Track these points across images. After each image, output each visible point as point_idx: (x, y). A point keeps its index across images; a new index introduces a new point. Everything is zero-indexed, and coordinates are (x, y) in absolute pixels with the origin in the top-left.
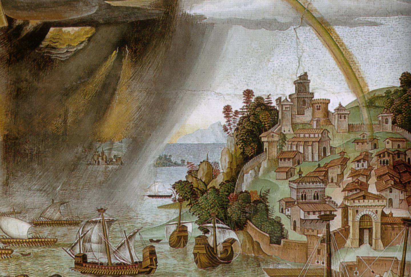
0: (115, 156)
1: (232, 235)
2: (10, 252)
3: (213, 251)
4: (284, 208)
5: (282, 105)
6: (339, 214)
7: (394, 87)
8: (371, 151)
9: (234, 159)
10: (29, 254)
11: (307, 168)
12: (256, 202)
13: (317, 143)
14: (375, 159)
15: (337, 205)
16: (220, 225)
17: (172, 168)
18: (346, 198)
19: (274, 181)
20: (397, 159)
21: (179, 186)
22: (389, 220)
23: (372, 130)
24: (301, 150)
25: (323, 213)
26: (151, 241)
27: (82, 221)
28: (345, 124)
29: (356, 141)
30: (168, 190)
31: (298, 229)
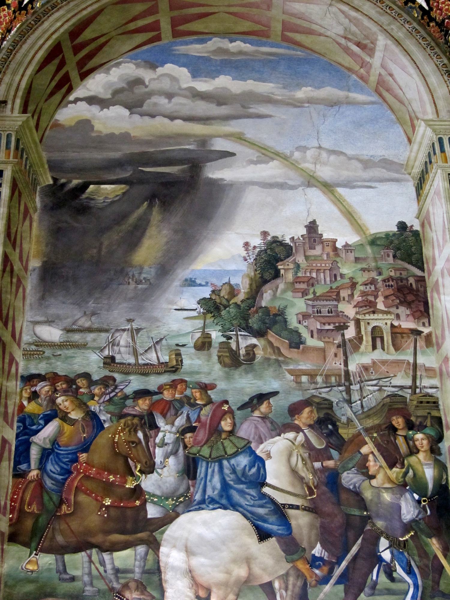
0: (144, 278)
1: (254, 341)
2: (41, 353)
4: (301, 319)
5: (295, 243)
6: (352, 326)
7: (391, 231)
8: (377, 278)
9: (254, 282)
10: (60, 355)
11: (320, 290)
12: (275, 315)
13: (328, 271)
14: (380, 284)
15: (350, 318)
16: (243, 333)
19: (291, 299)
20: (400, 284)
21: (203, 302)
24: (314, 275)
25: (337, 325)
26: (177, 345)
27: (111, 329)
28: (352, 256)
29: (363, 270)
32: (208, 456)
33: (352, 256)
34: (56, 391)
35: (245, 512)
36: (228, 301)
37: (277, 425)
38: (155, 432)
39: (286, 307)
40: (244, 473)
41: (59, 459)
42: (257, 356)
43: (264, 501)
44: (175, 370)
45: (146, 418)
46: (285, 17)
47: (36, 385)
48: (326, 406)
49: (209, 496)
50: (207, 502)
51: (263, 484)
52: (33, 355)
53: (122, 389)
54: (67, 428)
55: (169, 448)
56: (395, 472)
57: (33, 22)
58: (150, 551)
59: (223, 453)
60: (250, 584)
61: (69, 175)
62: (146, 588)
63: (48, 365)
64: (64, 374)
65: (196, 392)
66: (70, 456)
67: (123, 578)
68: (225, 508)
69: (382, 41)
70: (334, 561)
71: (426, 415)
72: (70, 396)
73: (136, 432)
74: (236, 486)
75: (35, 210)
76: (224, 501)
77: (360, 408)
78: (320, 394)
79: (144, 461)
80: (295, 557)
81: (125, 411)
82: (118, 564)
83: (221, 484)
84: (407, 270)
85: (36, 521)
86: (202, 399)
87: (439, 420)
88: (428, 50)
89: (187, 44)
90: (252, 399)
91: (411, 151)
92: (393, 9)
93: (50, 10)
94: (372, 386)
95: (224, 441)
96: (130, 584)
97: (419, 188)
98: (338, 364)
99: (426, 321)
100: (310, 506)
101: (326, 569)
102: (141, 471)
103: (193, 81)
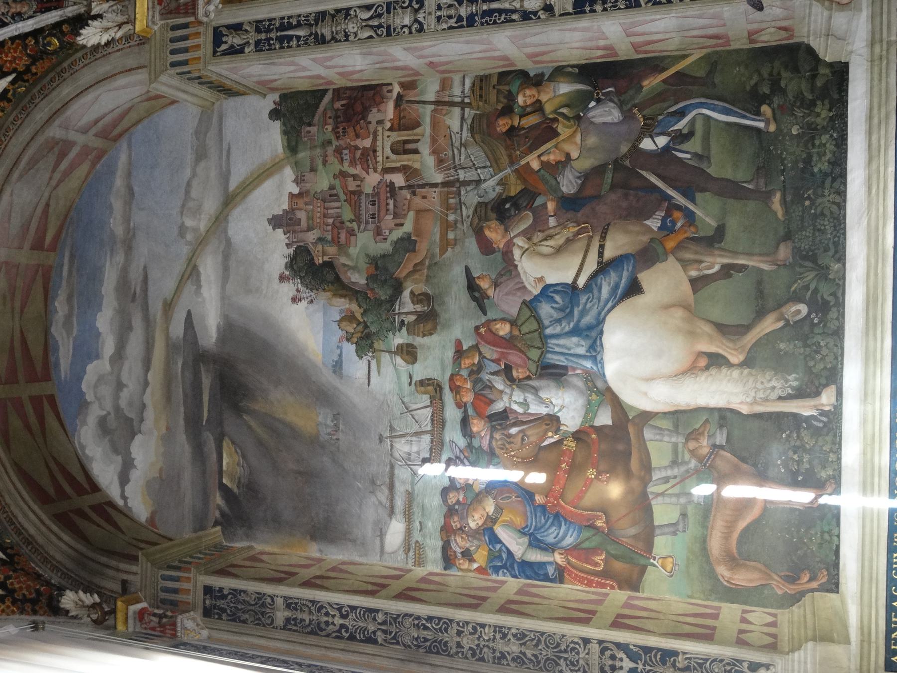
1: (406, 294)
3: (422, 315)
4: (382, 237)
6: (388, 178)
8: (334, 146)
10: (420, 523)
11: (347, 214)
12: (377, 268)
14: (341, 142)
16: (397, 307)
17: (344, 359)
18: (375, 171)
20: (342, 119)
22: (396, 122)
23: (316, 146)
24: (331, 221)
25: (388, 195)
26: (410, 384)
28: (309, 176)
29: (325, 162)
30: (363, 364)
31: (402, 221)
32: (539, 352)
33: (309, 176)
34: (461, 529)
35: (606, 309)
36: (359, 323)
37: (503, 269)
38: (511, 413)
39: (367, 255)
40: (561, 309)
41: (542, 527)
42: (423, 290)
43: (594, 286)
44: (438, 388)
45: (494, 423)
46: (27, 245)
47: (455, 552)
48: (483, 211)
49: (587, 352)
50: (594, 354)
51: (573, 286)
52: (420, 555)
53: (461, 451)
54: (506, 517)
55: (530, 397)
56: (563, 130)
57: (30, 548)
58: (651, 422)
59: (536, 334)
60: (693, 306)
61: (212, 506)
62: (695, 429)
63: (432, 537)
64: (442, 519)
65: (465, 364)
66: (538, 515)
67: (683, 456)
68: (602, 332)
69: (55, 131)
70: (666, 205)
71: (496, 91)
72: (468, 512)
73: (510, 436)
74: (575, 319)
75: (251, 548)
76: (593, 334)
77: (486, 170)
78: (469, 217)
79: (545, 427)
80: (660, 250)
81: (485, 446)
82: (666, 462)
83: (574, 336)
84: (325, 110)
85: (616, 558)
86: (474, 355)
87: (503, 75)
88: (65, 75)
89: (57, 364)
90: (475, 299)
91: (186, 101)
92: (17, 116)
93: (16, 527)
94: (460, 156)
95: (522, 332)
96: (691, 448)
97: (227, 91)
98: (434, 195)
99: (385, 89)
100: (600, 232)
101: (677, 214)
102: (557, 431)
103: (102, 358)
